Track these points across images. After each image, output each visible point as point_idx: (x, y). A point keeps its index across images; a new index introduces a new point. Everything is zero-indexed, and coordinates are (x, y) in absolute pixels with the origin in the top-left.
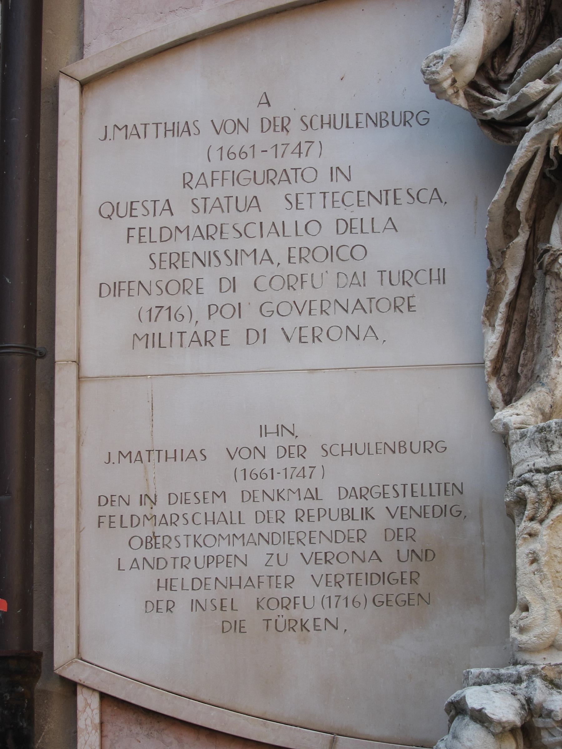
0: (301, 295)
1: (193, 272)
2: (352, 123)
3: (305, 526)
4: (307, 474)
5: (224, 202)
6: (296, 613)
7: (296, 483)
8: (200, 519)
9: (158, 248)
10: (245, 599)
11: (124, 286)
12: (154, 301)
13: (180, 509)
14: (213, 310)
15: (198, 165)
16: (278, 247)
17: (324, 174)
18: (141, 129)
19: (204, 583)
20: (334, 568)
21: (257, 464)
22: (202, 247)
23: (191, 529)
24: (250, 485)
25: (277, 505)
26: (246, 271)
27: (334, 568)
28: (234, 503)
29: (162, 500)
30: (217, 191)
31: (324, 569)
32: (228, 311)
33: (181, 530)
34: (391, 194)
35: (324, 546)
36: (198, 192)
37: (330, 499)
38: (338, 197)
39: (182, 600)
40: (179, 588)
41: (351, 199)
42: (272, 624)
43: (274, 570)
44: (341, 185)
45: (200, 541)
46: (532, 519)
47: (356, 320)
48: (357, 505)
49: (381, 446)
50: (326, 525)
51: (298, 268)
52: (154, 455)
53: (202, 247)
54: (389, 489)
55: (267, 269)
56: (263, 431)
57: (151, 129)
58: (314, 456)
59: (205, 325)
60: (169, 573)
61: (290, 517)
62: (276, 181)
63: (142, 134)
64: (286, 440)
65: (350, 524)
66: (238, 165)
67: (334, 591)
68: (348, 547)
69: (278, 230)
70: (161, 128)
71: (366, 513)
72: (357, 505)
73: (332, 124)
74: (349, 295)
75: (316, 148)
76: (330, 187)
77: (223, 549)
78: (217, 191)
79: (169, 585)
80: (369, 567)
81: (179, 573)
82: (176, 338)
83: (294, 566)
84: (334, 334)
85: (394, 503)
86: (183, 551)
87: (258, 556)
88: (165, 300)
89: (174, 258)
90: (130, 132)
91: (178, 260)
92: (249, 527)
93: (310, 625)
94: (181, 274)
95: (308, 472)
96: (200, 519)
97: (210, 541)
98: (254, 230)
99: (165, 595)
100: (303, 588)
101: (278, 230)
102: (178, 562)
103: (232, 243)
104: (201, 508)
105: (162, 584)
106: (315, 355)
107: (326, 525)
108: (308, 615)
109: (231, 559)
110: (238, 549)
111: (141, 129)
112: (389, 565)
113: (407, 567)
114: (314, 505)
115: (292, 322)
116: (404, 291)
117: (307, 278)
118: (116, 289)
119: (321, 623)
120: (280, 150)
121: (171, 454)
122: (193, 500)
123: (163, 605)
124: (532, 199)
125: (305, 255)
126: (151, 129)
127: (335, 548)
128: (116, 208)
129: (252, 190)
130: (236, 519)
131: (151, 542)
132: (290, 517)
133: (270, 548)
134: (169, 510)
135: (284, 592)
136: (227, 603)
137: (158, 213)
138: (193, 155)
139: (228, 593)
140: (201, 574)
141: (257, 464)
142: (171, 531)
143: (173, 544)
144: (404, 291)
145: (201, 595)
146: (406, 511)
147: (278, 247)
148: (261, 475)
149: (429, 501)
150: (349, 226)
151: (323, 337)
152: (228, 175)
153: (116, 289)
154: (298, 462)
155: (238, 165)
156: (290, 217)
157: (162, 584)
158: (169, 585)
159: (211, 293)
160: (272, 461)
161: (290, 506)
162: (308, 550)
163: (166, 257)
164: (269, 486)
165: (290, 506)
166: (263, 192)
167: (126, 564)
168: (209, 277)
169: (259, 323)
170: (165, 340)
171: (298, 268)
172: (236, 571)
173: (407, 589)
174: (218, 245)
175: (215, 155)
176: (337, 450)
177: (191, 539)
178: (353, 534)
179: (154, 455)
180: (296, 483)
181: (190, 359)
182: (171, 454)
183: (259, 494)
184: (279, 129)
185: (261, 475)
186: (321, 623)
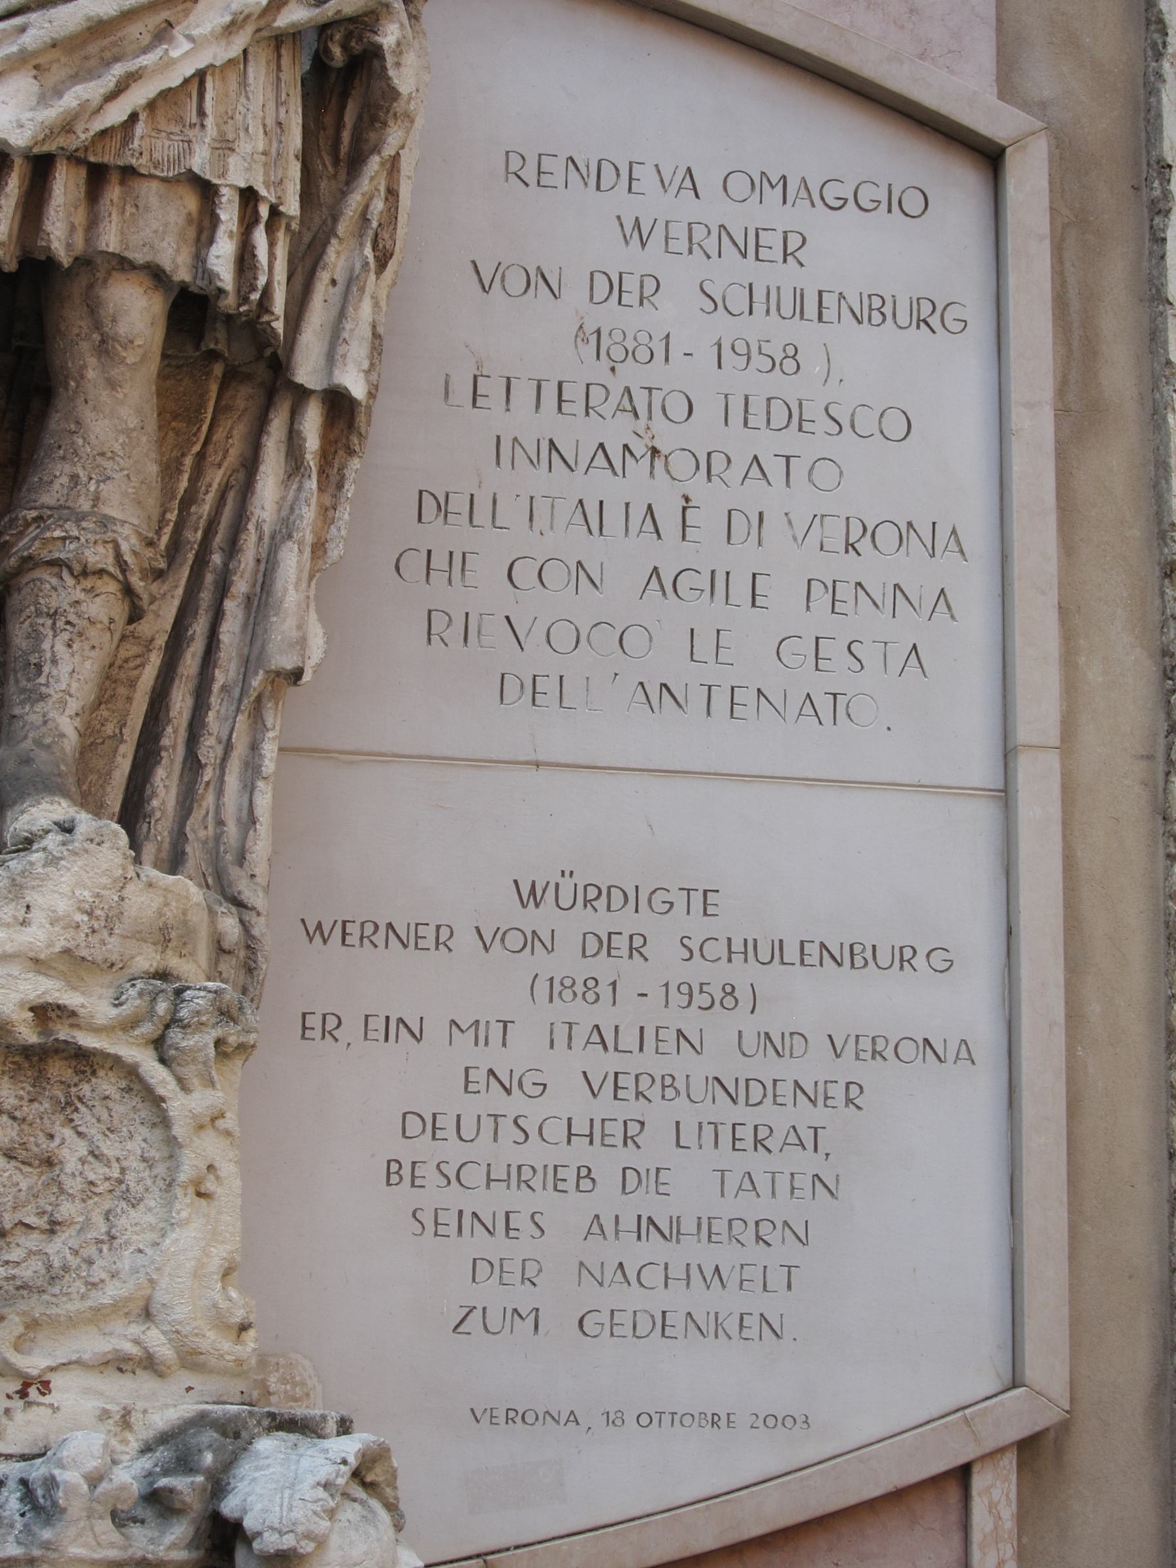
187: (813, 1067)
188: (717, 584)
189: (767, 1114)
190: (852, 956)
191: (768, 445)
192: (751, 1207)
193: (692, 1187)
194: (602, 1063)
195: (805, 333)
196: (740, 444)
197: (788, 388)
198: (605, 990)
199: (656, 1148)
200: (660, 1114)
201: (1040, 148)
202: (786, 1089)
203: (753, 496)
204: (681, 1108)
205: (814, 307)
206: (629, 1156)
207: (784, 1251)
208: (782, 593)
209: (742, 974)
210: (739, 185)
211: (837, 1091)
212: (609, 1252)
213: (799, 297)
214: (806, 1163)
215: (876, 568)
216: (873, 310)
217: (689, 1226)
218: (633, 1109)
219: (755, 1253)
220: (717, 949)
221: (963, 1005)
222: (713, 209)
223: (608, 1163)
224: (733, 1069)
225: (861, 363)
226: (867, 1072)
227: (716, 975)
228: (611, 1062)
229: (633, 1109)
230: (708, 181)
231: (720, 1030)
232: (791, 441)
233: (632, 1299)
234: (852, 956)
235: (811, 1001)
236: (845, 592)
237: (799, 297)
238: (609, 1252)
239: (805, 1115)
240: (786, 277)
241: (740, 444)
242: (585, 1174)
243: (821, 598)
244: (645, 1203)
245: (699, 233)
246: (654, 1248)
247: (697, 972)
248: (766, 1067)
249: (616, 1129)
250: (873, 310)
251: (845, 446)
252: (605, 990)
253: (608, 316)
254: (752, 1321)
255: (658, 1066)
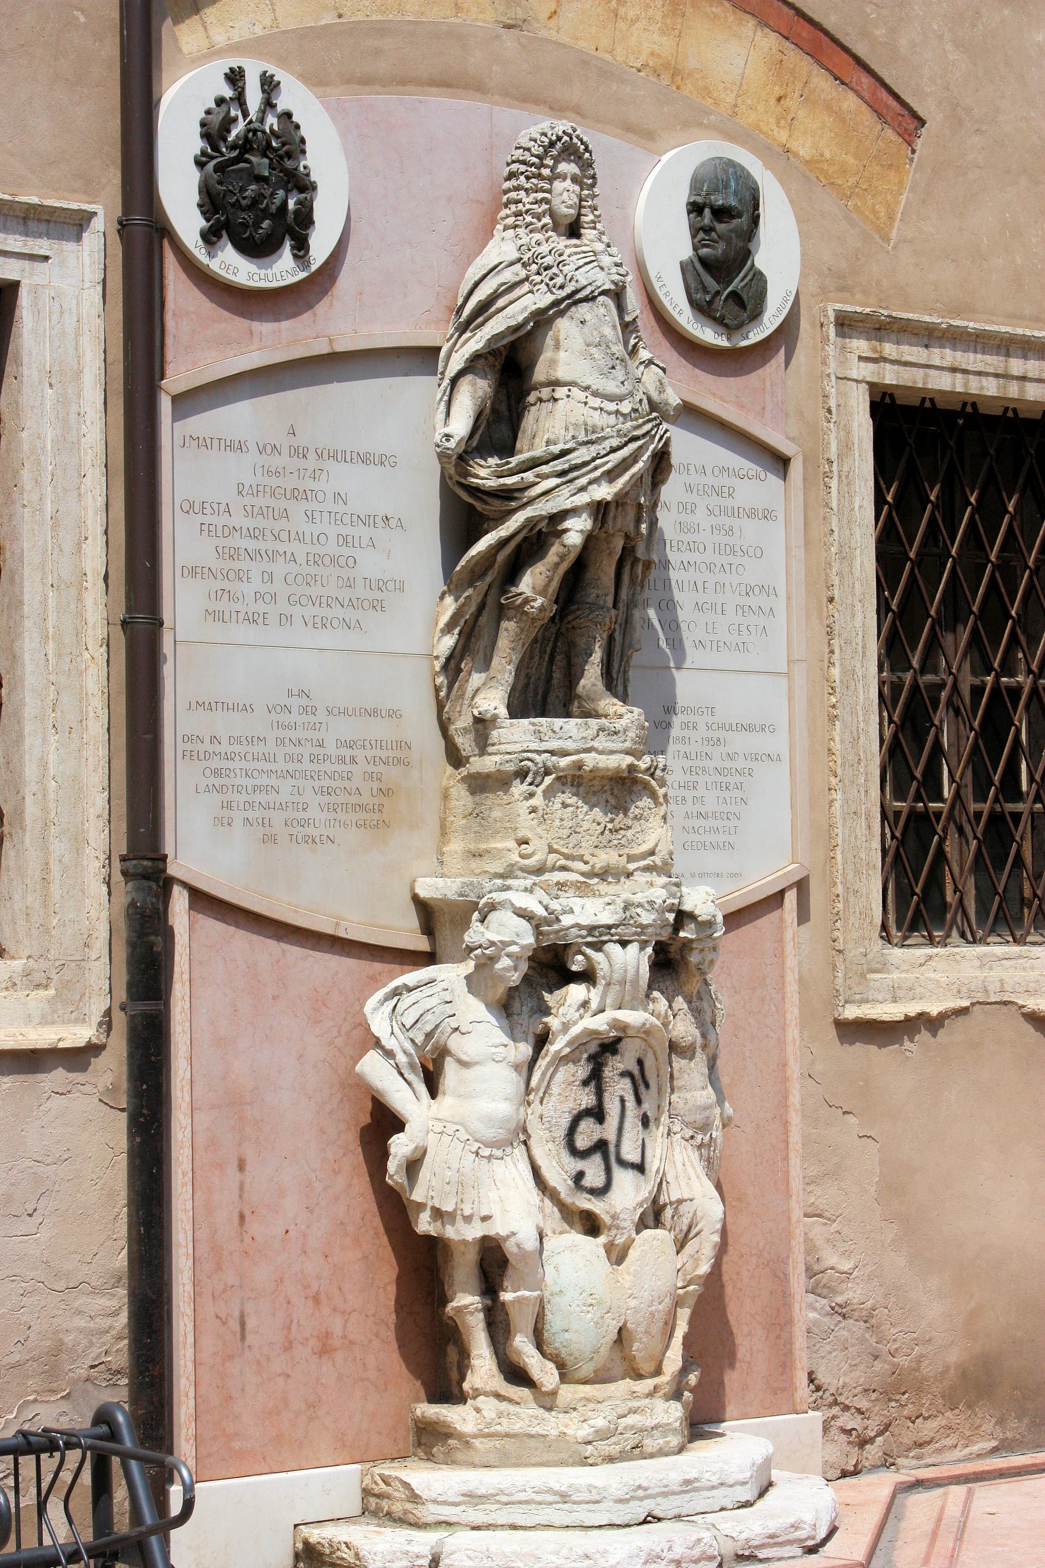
0: (315, 591)
1: (244, 564)
2: (348, 459)
3: (315, 767)
4: (317, 728)
5: (265, 510)
6: (310, 831)
7: (309, 734)
8: (249, 757)
9: (221, 542)
10: (278, 818)
11: (199, 570)
12: (219, 584)
13: (237, 748)
14: (258, 596)
15: (248, 479)
16: (300, 550)
17: (330, 497)
18: (208, 441)
19: (251, 805)
20: (332, 799)
21: (285, 718)
22: (252, 545)
23: (243, 764)
24: (282, 733)
25: (298, 750)
26: (280, 568)
27: (332, 799)
28: (271, 747)
29: (225, 741)
30: (261, 501)
31: (326, 799)
32: (268, 598)
33: (237, 764)
34: (372, 518)
35: (326, 782)
36: (248, 500)
37: (331, 749)
38: (338, 517)
39: (238, 816)
40: (235, 808)
41: (347, 519)
42: (294, 837)
43: (295, 799)
44: (340, 508)
45: (249, 774)
46: (531, 784)
47: (350, 614)
48: (347, 753)
49: (363, 711)
50: (328, 767)
51: (313, 570)
52: (220, 705)
53: (252, 545)
54: (367, 743)
55: (293, 568)
56: (290, 693)
57: (216, 442)
58: (321, 715)
59: (253, 607)
60: (230, 796)
61: (306, 759)
62: (299, 498)
63: (209, 446)
64: (304, 701)
65: (343, 767)
66: (274, 482)
67: (333, 815)
68: (342, 784)
69: (300, 538)
70: (222, 442)
71: (353, 760)
72: (347, 753)
73: (335, 457)
74: (345, 595)
75: (324, 475)
76: (334, 508)
77: (263, 780)
78: (261, 501)
79: (229, 806)
80: (354, 799)
81: (236, 797)
82: (234, 615)
83: (309, 797)
84: (335, 623)
85: (370, 753)
86: (238, 781)
87: (286, 786)
88: (227, 585)
89: (232, 551)
90: (203, 443)
91: (233, 555)
92: (281, 765)
93: (317, 840)
94: (236, 565)
95: (318, 726)
96: (249, 757)
97: (255, 773)
98: (284, 536)
99: (226, 813)
100: (314, 812)
101: (300, 538)
102: (235, 788)
103: (270, 545)
104: (250, 749)
105: (225, 805)
106: (324, 638)
107: (328, 767)
108: (316, 833)
109: (269, 788)
110: (273, 781)
111: (208, 441)
112: (366, 799)
113: (376, 801)
114: (321, 751)
115: (309, 611)
116: (378, 595)
117: (318, 578)
118: (193, 572)
119: (324, 838)
120: (302, 472)
121: (231, 707)
122: (245, 742)
123: (225, 821)
124: (509, 556)
125: (316, 560)
126: (216, 442)
127: (334, 784)
128: (192, 505)
129: (283, 504)
130: (272, 760)
131: (217, 773)
132: (306, 759)
133: (293, 782)
134: (230, 749)
135: (302, 815)
136: (266, 821)
137: (221, 512)
138: (243, 469)
139: (267, 814)
140: (250, 798)
141: (285, 718)
142: (230, 764)
143: (232, 775)
144: (378, 595)
145: (250, 814)
146: (377, 759)
147: (300, 550)
148: (288, 727)
149: (390, 753)
150: (345, 540)
151: (328, 625)
152: (268, 489)
153: (193, 572)
154: (311, 718)
155: (274, 482)
156: (308, 528)
157: (225, 805)
158: (229, 806)
159: (256, 583)
160: (294, 717)
161: (307, 750)
162: (317, 784)
163: (226, 550)
164: (293, 735)
165: (307, 750)
166: (292, 506)
167: (201, 789)
168: (255, 569)
169: (289, 610)
170: (227, 617)
171: (313, 570)
172: (271, 797)
173: (376, 817)
174: (261, 545)
175: (259, 471)
176: (335, 711)
177: (244, 772)
178: (345, 774)
179: (220, 705)
180: (309, 734)
181: (243, 633)
182: (231, 707)
183: (287, 741)
184: (301, 456)
185: (288, 727)
186: (324, 838)
187: (740, 764)
188: (713, 607)
189: (729, 779)
190: (749, 728)
191: (725, 560)
192: (726, 808)
193: (711, 804)
194: (688, 764)
195: (735, 522)
196: (719, 560)
197: (731, 541)
198: (687, 740)
199: (701, 791)
200: (702, 779)
201: (800, 458)
202: (733, 770)
203: (721, 577)
204: (707, 778)
205: (735, 513)
206: (694, 793)
207: (735, 822)
208: (730, 609)
209: (721, 734)
210: (716, 470)
211: (746, 771)
212: (689, 823)
213: (733, 508)
214: (738, 794)
215: (753, 601)
216: (752, 514)
217: (710, 815)
218: (695, 778)
219: (726, 822)
220: (715, 727)
221: (778, 743)
222: (709, 480)
223: (689, 795)
224: (720, 764)
225: (750, 530)
226: (754, 765)
227: (715, 735)
228: (689, 763)
229: (695, 778)
230: (708, 471)
231: (716, 752)
232: (731, 559)
233: (696, 837)
234: (749, 728)
235: (740, 742)
236: (746, 609)
237: (733, 508)
238: (689, 823)
239: (738, 779)
240: (729, 502)
241: (719, 560)
242: (684, 799)
243: (740, 611)
244: (699, 808)
245: (706, 487)
246: (701, 822)
247: (710, 734)
248: (728, 764)
249: (690, 784)
250: (752, 514)
251: (745, 560)
252: (687, 740)
253: (683, 517)
254: (726, 844)
255: (701, 764)
